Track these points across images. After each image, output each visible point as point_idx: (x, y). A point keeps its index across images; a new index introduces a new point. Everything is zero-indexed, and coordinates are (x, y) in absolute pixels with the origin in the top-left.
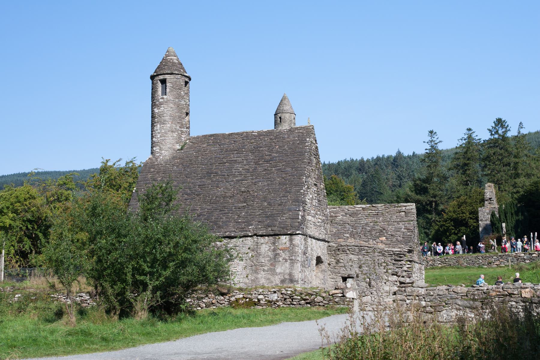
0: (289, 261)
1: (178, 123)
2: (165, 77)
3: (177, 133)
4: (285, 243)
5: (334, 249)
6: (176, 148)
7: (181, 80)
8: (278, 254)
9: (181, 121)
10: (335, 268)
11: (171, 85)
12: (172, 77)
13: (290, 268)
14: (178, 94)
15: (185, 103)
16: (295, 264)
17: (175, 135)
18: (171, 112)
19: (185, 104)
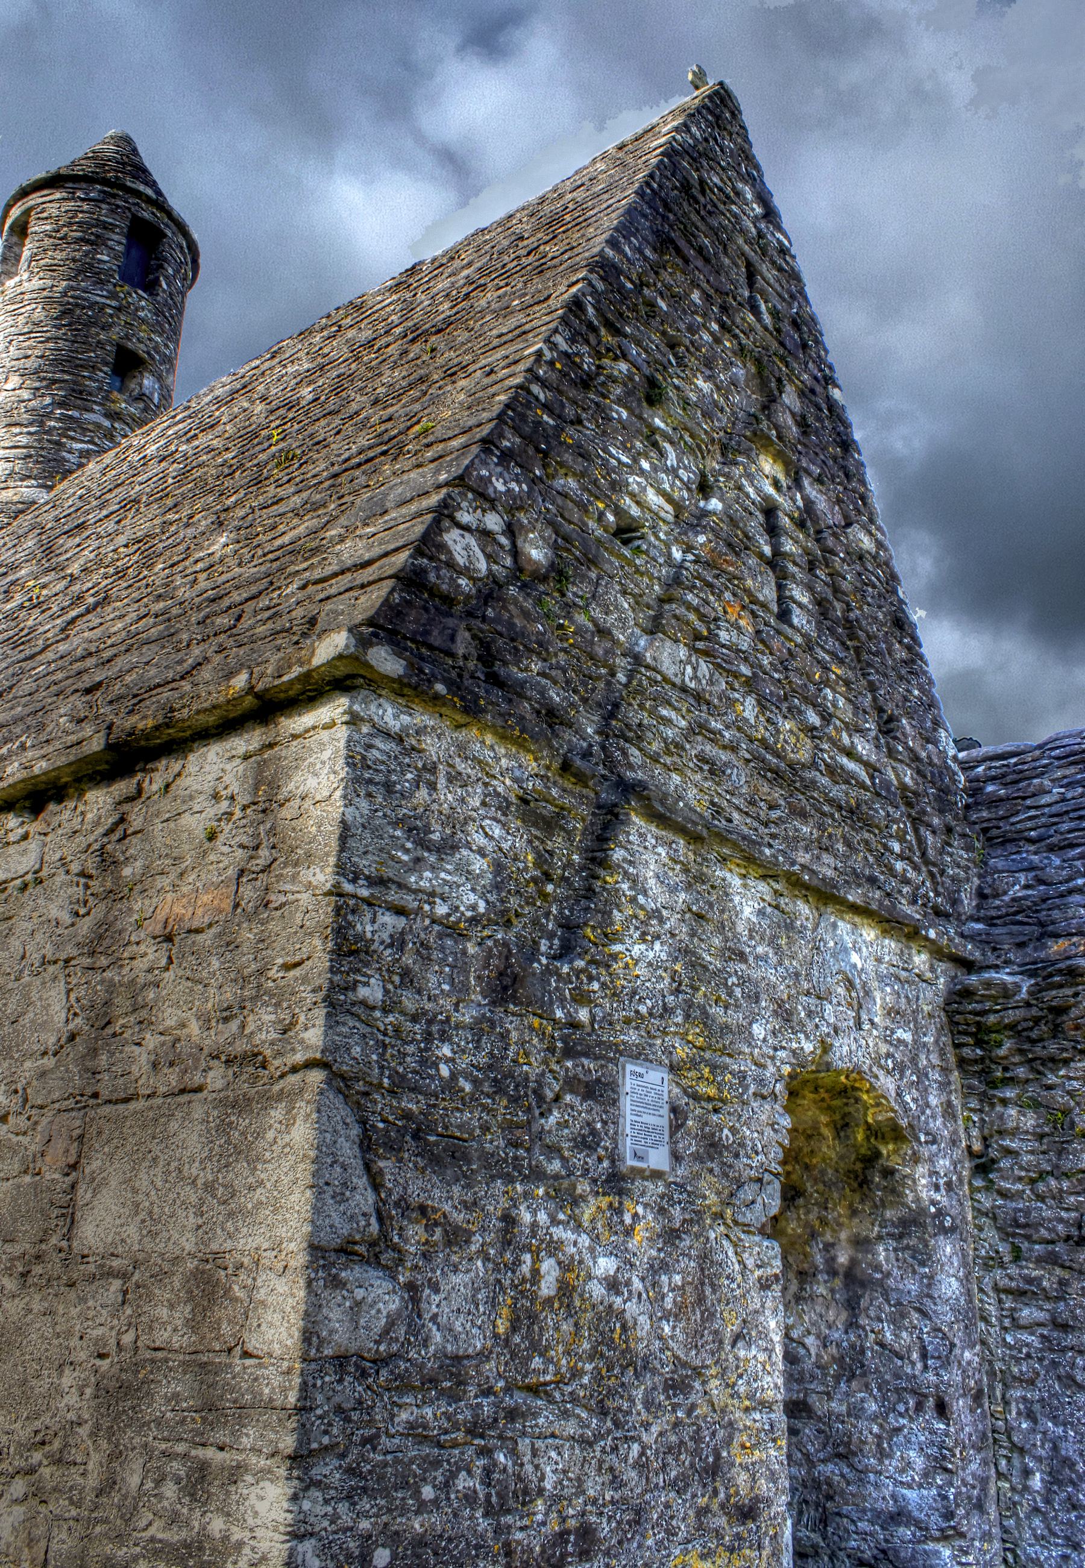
0: (216, 1078)
1: (54, 381)
2: (32, 203)
3: (32, 429)
4: (212, 837)
5: (1011, 1016)
6: (16, 499)
7: (104, 206)
8: (134, 989)
9: (67, 377)
10: (1041, 1187)
11: (48, 227)
12: (58, 195)
13: (210, 1187)
14: (74, 260)
15: (114, 303)
16: (277, 1113)
17: (24, 440)
18: (21, 338)
19: (119, 309)
